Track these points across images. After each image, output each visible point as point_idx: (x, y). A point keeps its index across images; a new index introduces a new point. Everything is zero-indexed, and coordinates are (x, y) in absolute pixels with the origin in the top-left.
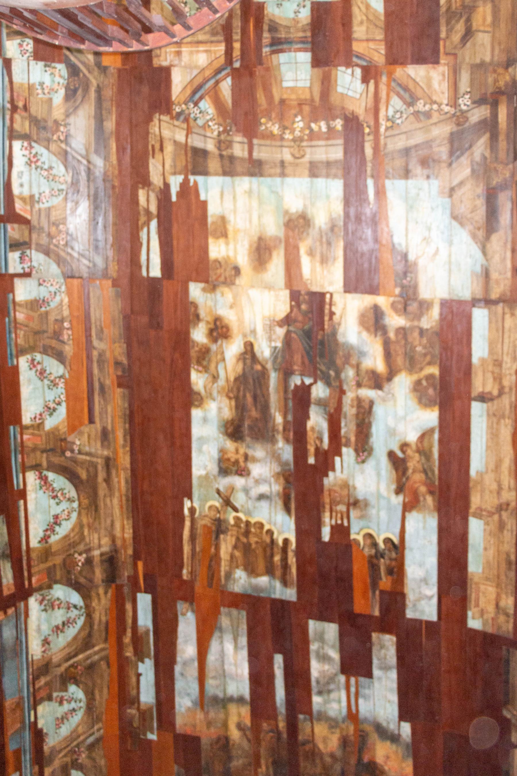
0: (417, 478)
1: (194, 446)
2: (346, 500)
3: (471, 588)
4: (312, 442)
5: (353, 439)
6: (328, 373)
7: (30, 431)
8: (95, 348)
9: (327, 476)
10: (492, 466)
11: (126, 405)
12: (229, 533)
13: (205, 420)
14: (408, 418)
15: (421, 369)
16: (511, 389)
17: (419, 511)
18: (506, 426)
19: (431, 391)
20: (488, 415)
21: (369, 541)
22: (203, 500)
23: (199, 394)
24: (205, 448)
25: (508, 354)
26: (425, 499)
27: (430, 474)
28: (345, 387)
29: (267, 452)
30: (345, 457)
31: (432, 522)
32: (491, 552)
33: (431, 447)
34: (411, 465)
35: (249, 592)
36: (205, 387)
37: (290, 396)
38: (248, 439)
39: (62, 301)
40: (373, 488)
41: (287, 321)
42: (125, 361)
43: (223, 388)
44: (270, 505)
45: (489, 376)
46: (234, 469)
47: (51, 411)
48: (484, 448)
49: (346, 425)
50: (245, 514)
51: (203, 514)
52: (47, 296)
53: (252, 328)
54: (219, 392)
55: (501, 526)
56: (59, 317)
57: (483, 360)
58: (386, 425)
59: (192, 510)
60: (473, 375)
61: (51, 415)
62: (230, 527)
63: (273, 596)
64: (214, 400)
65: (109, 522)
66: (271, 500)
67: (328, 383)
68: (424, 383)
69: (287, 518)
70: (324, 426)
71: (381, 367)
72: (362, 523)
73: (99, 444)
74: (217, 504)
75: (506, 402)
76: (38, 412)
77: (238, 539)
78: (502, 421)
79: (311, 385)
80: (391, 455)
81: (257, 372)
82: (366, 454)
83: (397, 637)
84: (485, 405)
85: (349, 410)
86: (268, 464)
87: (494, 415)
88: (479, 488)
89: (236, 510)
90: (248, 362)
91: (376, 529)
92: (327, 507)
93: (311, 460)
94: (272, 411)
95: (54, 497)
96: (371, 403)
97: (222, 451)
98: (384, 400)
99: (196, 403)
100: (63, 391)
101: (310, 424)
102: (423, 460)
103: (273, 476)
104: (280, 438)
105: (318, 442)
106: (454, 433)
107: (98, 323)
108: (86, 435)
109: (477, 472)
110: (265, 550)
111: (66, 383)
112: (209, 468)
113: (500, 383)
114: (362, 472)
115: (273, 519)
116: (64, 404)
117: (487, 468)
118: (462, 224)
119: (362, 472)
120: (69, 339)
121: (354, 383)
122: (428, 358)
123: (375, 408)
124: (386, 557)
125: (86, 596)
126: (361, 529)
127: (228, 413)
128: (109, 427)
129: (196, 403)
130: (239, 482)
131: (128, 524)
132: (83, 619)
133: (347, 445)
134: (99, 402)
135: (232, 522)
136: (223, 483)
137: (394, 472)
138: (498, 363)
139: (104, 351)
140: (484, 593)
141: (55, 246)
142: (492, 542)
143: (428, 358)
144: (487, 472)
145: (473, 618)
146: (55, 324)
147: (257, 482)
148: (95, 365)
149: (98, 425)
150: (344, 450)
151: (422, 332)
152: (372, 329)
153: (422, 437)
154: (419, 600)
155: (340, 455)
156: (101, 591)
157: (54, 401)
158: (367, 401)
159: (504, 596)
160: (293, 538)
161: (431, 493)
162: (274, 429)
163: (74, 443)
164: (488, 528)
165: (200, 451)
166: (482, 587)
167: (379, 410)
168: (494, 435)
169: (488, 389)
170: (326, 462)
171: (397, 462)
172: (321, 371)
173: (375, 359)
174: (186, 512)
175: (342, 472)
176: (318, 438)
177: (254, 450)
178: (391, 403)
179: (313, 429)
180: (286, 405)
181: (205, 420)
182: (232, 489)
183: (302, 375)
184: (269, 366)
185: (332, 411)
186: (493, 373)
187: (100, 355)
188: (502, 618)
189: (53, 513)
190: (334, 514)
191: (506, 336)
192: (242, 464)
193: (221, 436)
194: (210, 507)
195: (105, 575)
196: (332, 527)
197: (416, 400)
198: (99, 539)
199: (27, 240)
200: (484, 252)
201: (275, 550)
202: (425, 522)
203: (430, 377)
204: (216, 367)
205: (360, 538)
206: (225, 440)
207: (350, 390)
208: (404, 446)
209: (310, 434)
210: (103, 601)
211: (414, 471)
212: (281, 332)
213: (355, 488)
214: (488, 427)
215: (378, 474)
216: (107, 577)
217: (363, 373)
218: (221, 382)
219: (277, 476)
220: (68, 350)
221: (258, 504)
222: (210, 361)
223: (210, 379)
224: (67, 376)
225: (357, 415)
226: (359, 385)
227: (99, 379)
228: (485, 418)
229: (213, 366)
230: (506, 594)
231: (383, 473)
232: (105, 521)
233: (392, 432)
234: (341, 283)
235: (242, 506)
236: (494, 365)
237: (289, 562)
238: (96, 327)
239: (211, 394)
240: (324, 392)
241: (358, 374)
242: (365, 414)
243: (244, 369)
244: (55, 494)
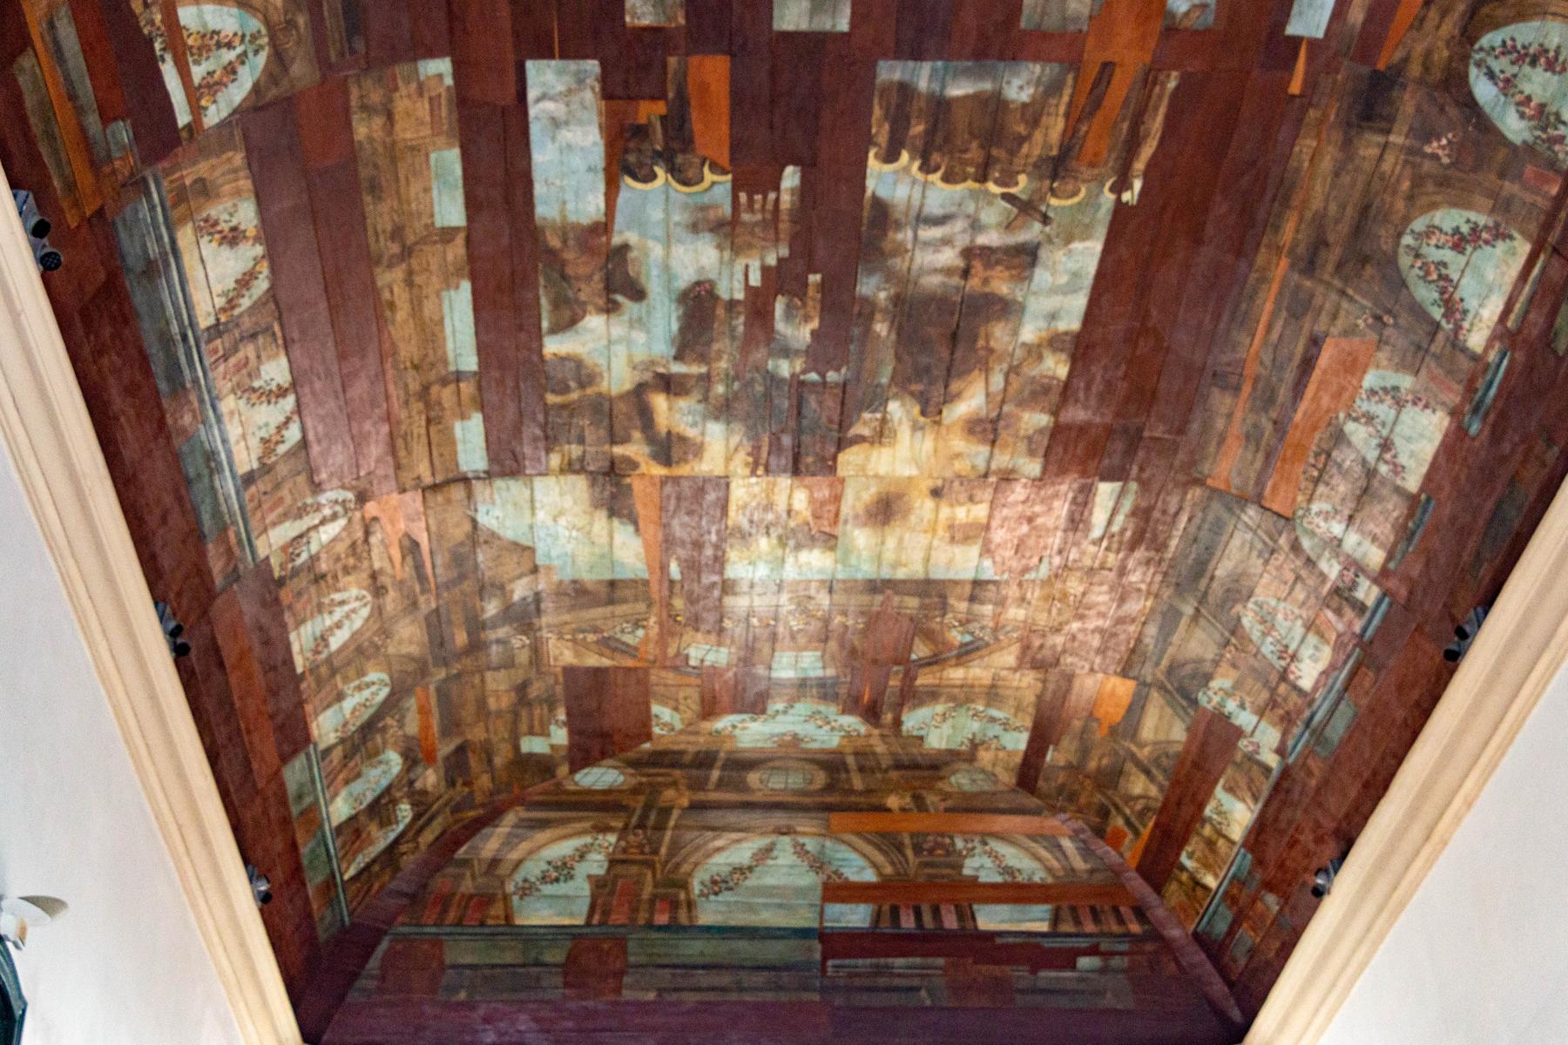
2: (739, 230)
3: (450, 123)
5: (720, 312)
9: (780, 260)
12: (1031, 160)
14: (605, 342)
17: (576, 227)
21: (690, 174)
22: (1091, 203)
26: (565, 242)
27: (556, 275)
31: (545, 209)
32: (415, 188)
34: (597, 283)
35: (1001, 65)
41: (842, 444)
44: (922, 206)
48: (447, 321)
50: (987, 192)
51: (1093, 185)
53: (919, 434)
55: (397, 233)
58: (648, 332)
59: (1118, 188)
62: (1030, 168)
63: (939, 63)
65: (1346, 179)
66: (918, 216)
69: (883, 193)
70: (780, 325)
71: (659, 402)
72: (706, 199)
74: (1054, 202)
76: (1417, 409)
77: (1013, 153)
80: (638, 294)
83: (624, 24)
84: (452, 368)
86: (915, 267)
88: (451, 269)
89: (1005, 197)
91: (672, 194)
92: (784, 217)
93: (815, 278)
95: (1447, 278)
96: (678, 357)
102: (570, 294)
103: (907, 251)
109: (457, 287)
110: (947, 140)
115: (918, 190)
118: (516, 544)
123: (673, 352)
124: (650, 153)
125: (1454, 85)
126: (706, 190)
130: (991, 238)
131: (1300, 162)
132: (1486, 41)
133: (732, 304)
135: (1023, 179)
136: (1032, 232)
137: (631, 273)
140: (422, 123)
142: (413, 206)
145: (440, 76)
147: (946, 242)
150: (739, 296)
151: (581, 441)
152: (674, 439)
153: (573, 322)
154: (570, 91)
156: (1415, 70)
159: (378, 134)
160: (873, 164)
161: (552, 253)
164: (425, 220)
166: (429, 132)
168: (431, 333)
170: (779, 280)
173: (670, 409)
174: (1138, 185)
175: (747, 267)
177: (944, 284)
179: (807, 319)
182: (1009, 227)
188: (376, 97)
189: (1462, 260)
190: (770, 207)
194: (1075, 194)
195: (1395, 94)
196: (777, 189)
198: (1381, 158)
200: (474, 522)
201: (919, 143)
202: (562, 211)
205: (709, 176)
208: (611, 308)
210: (1419, 49)
211: (589, 278)
212: (859, 429)
213: (720, 247)
215: (666, 268)
216: (1391, 88)
221: (953, 209)
228: (451, 356)
230: (371, 139)
231: (655, 272)
232: (1353, 184)
233: (638, 323)
234: (733, 486)
235: (990, 204)
237: (887, 126)
244: (1442, 283)
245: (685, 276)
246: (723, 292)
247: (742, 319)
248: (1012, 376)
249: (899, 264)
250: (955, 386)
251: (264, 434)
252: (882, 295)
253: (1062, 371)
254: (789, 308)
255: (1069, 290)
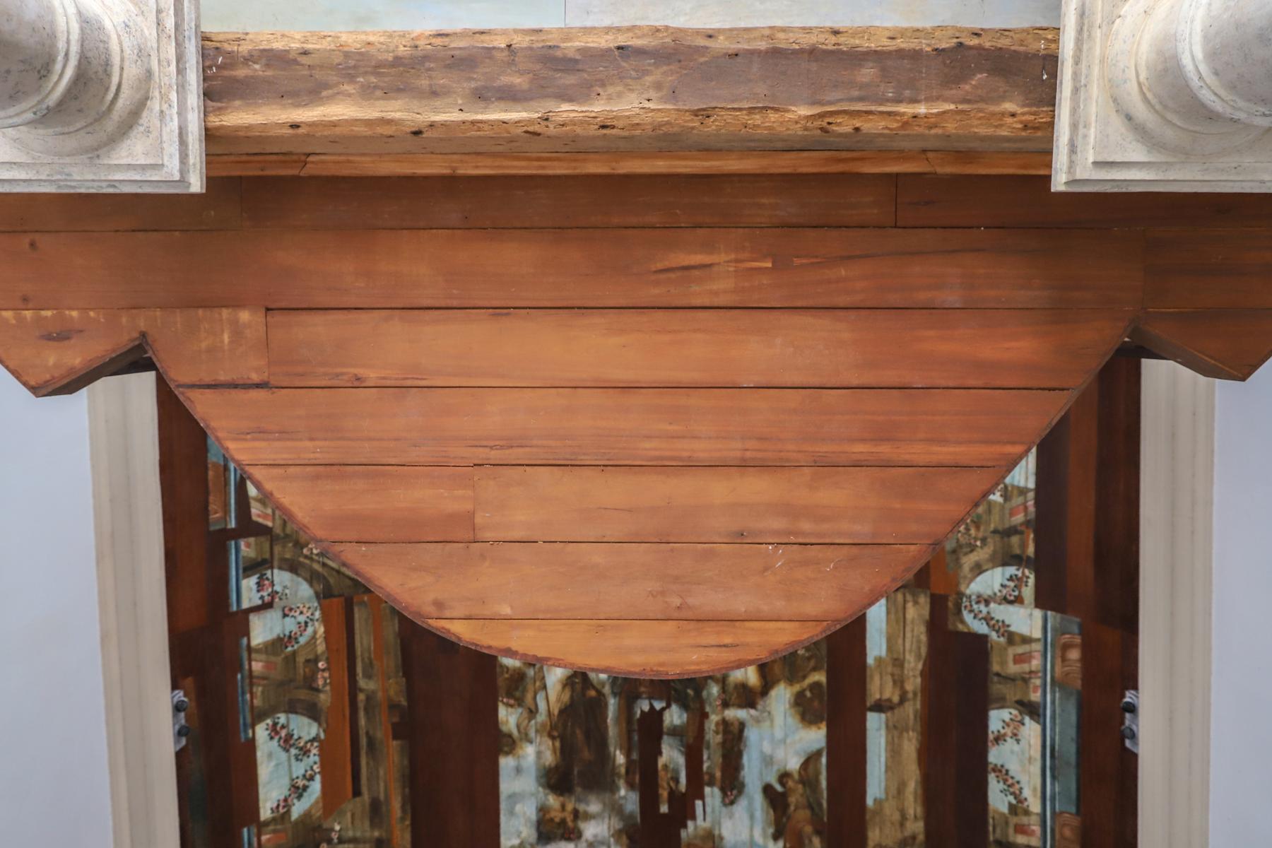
0: (800, 817)
1: (503, 806)
4: (665, 785)
5: (718, 774)
6: (687, 694)
7: (271, 827)
8: (361, 690)
9: (685, 826)
10: (893, 790)
11: (406, 762)
13: (518, 770)
14: (788, 741)
15: (804, 677)
16: (915, 694)
18: (910, 740)
19: (816, 704)
20: (887, 727)
23: (510, 736)
24: (518, 808)
25: (910, 651)
26: (811, 841)
28: (708, 709)
29: (604, 805)
30: (708, 800)
33: (818, 774)
34: (792, 800)
36: (518, 726)
37: (636, 727)
38: (578, 790)
39: (315, 632)
40: (745, 836)
42: (404, 703)
43: (543, 725)
45: (889, 680)
46: (560, 831)
47: (298, 791)
48: (883, 769)
49: (709, 758)
52: (294, 629)
54: (537, 731)
56: (311, 657)
57: (879, 660)
58: (762, 752)
60: (868, 680)
61: (300, 797)
64: (531, 742)
67: (685, 706)
68: (808, 694)
70: (681, 760)
73: (367, 823)
75: (911, 710)
78: (905, 735)
79: (663, 709)
80: (767, 790)
81: (591, 698)
82: (735, 792)
84: (883, 716)
85: (713, 737)
86: (606, 820)
87: (895, 727)
90: (578, 687)
93: (664, 809)
94: (612, 749)
96: (742, 725)
97: (542, 810)
98: (758, 721)
99: (506, 749)
100: (317, 759)
101: (662, 761)
103: (613, 836)
104: (621, 783)
105: (672, 784)
106: (846, 754)
107: (366, 655)
108: (349, 815)
109: (875, 800)
111: (321, 749)
112: (524, 835)
113: (902, 688)
114: (731, 816)
116: (318, 778)
117: (887, 793)
119: (731, 816)
120: (325, 684)
121: (718, 703)
122: (812, 663)
123: (746, 733)
127: (549, 759)
128: (382, 797)
129: (506, 749)
133: (711, 784)
134: (368, 764)
137: (771, 812)
138: (898, 662)
139: (374, 692)
141: (306, 557)
143: (812, 663)
144: (887, 799)
146: (305, 667)
148: (362, 714)
149: (366, 797)
150: (707, 790)
155: (702, 797)
157: (304, 776)
158: (736, 724)
161: (818, 832)
162: (614, 772)
163: (332, 830)
165: (512, 813)
167: (751, 734)
168: (894, 752)
169: (887, 695)
170: (683, 808)
171: (775, 799)
172: (676, 690)
176: (672, 778)
177: (587, 803)
178: (768, 723)
179: (665, 767)
180: (630, 738)
181: (518, 770)
183: (650, 698)
184: (607, 690)
185: (691, 740)
186: (893, 675)
187: (368, 698)
191: (908, 629)
192: (570, 824)
193: (541, 789)
197: (798, 717)
199: (267, 556)
203: (816, 686)
204: (535, 698)
206: (546, 795)
207: (714, 712)
208: (784, 777)
209: (661, 773)
213: (721, 838)
214: (887, 742)
215: (752, 817)
217: (730, 688)
218: (542, 717)
219: (617, 834)
220: (324, 699)
222: (525, 691)
223: (525, 715)
224: (322, 736)
225: (724, 744)
226: (726, 705)
227: (367, 733)
228: (883, 732)
229: (529, 696)
233: (768, 761)
236: (894, 665)
238: (363, 660)
239: (526, 735)
240: (680, 717)
241: (724, 690)
242: (734, 738)
243: (572, 697)
245: (740, 808)
246: (716, 791)
247: (705, 766)
248: (533, 708)
249: (617, 824)
250: (566, 697)
251: (1016, 748)
252: (623, 792)
253: (503, 712)
254: (677, 781)
255: (514, 797)
